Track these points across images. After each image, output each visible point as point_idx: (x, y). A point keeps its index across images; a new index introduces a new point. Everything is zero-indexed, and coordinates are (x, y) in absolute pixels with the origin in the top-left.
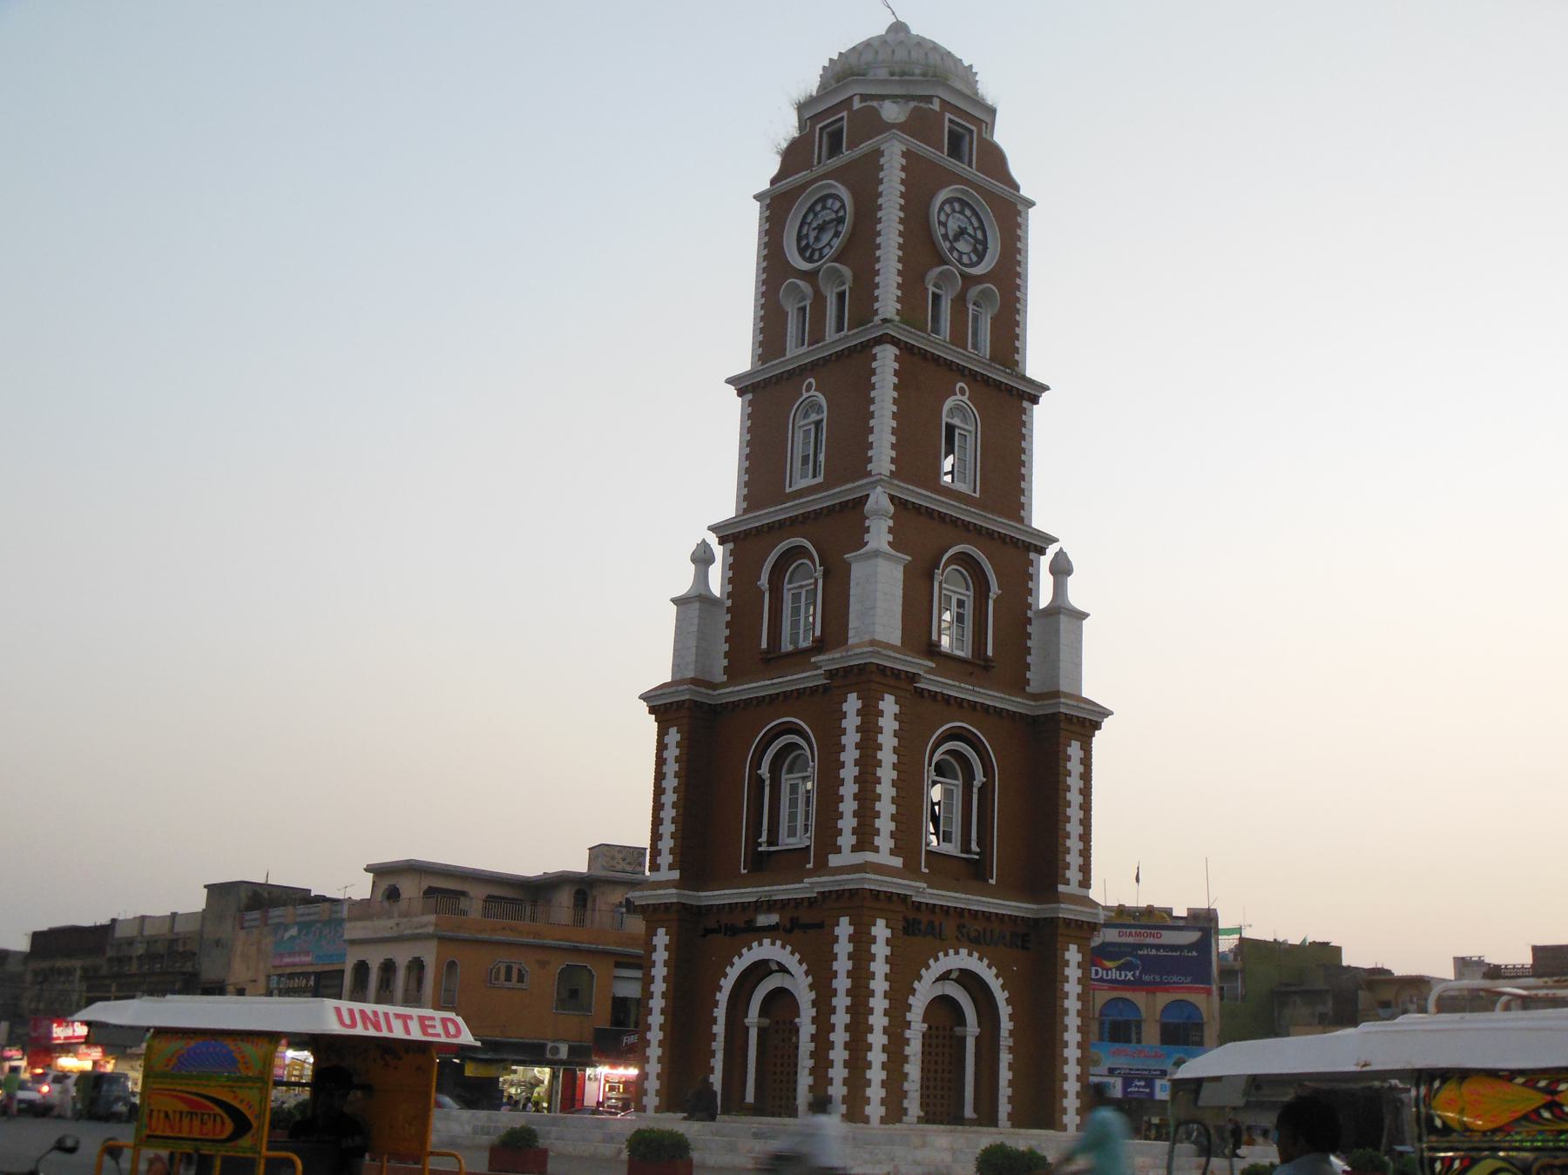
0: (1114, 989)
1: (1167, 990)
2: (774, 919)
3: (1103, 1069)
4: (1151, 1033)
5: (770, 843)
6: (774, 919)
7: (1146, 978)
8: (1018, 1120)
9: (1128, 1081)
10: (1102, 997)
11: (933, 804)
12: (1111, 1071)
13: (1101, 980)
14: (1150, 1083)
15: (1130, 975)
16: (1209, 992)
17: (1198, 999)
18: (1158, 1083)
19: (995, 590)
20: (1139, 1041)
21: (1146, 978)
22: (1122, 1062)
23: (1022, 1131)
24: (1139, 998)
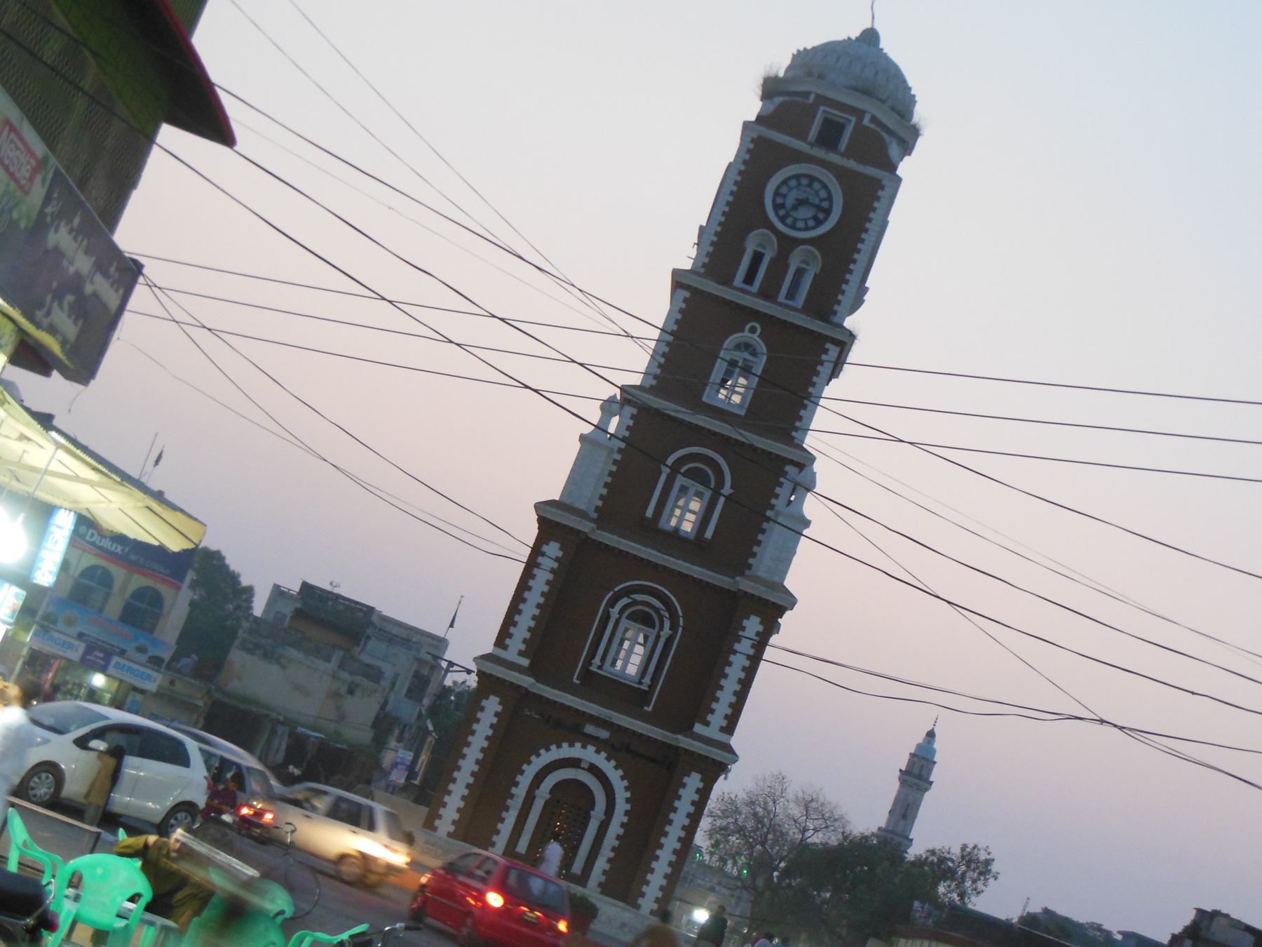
0: (97, 555)
1: (145, 575)
2: (604, 734)
3: (74, 631)
4: (115, 607)
5: (600, 668)
6: (604, 734)
7: (133, 557)
8: (605, 889)
9: (90, 649)
10: (89, 560)
11: (644, 645)
12: (81, 636)
13: (93, 544)
14: (108, 657)
15: (119, 549)
16: (178, 588)
17: (166, 591)
18: (115, 659)
19: (727, 490)
20: (101, 611)
21: (133, 557)
22: (94, 632)
23: (606, 898)
24: (118, 573)
